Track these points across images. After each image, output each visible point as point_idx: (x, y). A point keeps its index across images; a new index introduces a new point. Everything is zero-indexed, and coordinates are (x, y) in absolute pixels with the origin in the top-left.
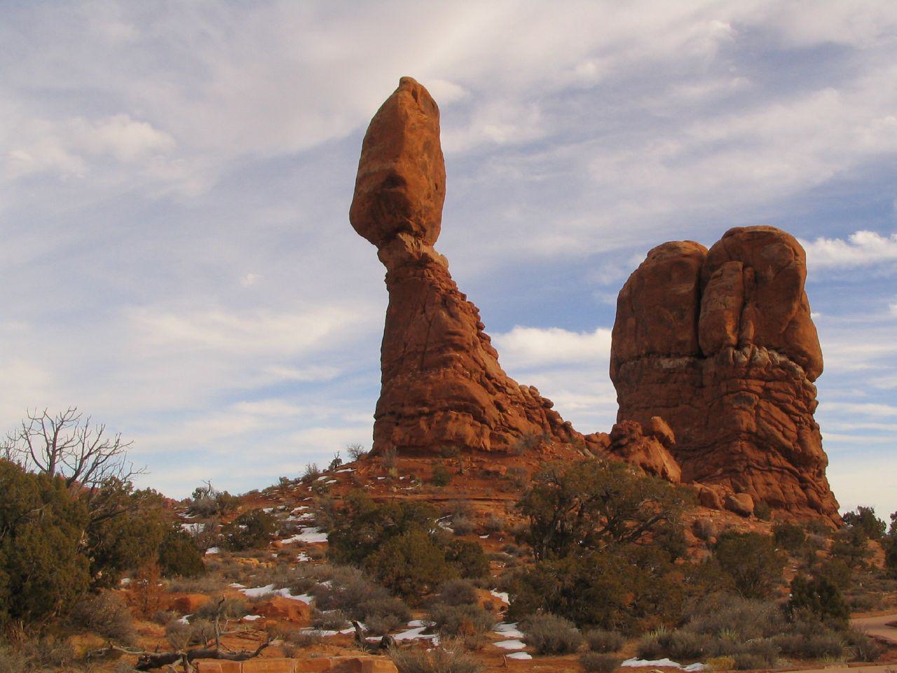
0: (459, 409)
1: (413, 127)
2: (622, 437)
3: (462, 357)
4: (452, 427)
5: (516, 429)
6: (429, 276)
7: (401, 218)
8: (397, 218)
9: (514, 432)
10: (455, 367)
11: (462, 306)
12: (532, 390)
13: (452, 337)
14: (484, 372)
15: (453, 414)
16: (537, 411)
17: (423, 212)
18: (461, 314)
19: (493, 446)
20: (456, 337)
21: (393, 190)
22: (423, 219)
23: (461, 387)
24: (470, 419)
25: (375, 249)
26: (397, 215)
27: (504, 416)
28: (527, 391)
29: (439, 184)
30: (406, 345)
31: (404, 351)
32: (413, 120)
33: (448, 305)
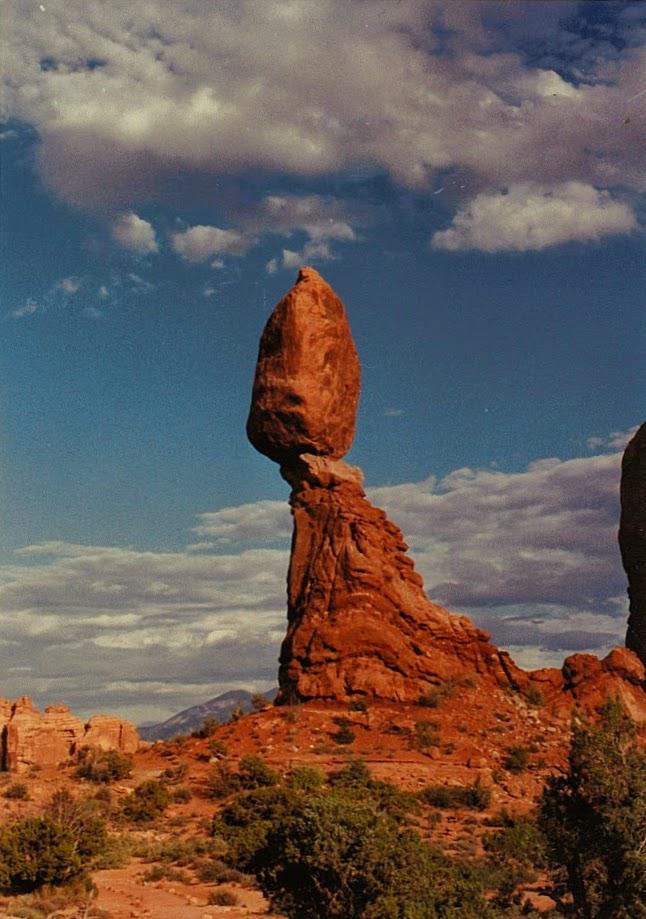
0: (369, 654)
2: (574, 673)
3: (372, 596)
4: (361, 677)
5: (435, 675)
6: (338, 501)
9: (433, 679)
10: (364, 608)
12: (463, 622)
13: (362, 575)
14: (397, 611)
15: (363, 660)
16: (469, 646)
18: (370, 549)
19: (408, 696)
23: (371, 631)
24: (380, 666)
27: (422, 661)
28: (457, 623)
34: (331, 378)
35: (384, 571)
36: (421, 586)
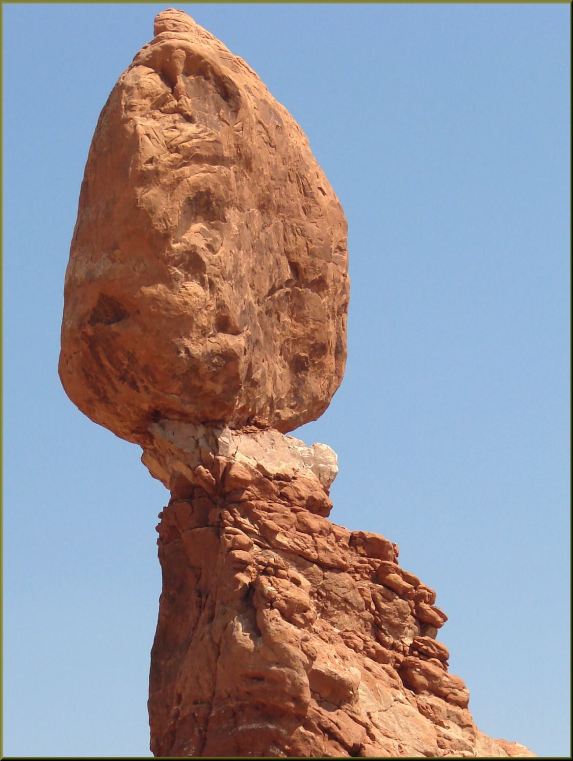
1: (150, 167)
6: (237, 524)
7: (146, 388)
8: (137, 388)
11: (283, 604)
17: (204, 368)
20: (265, 685)
21: (114, 327)
22: (209, 385)
25: (137, 450)
26: (139, 384)
29: (303, 259)
30: (180, 696)
31: (177, 715)
32: (150, 148)
33: (255, 603)
34: (206, 256)
35: (317, 677)
36: (463, 705)
